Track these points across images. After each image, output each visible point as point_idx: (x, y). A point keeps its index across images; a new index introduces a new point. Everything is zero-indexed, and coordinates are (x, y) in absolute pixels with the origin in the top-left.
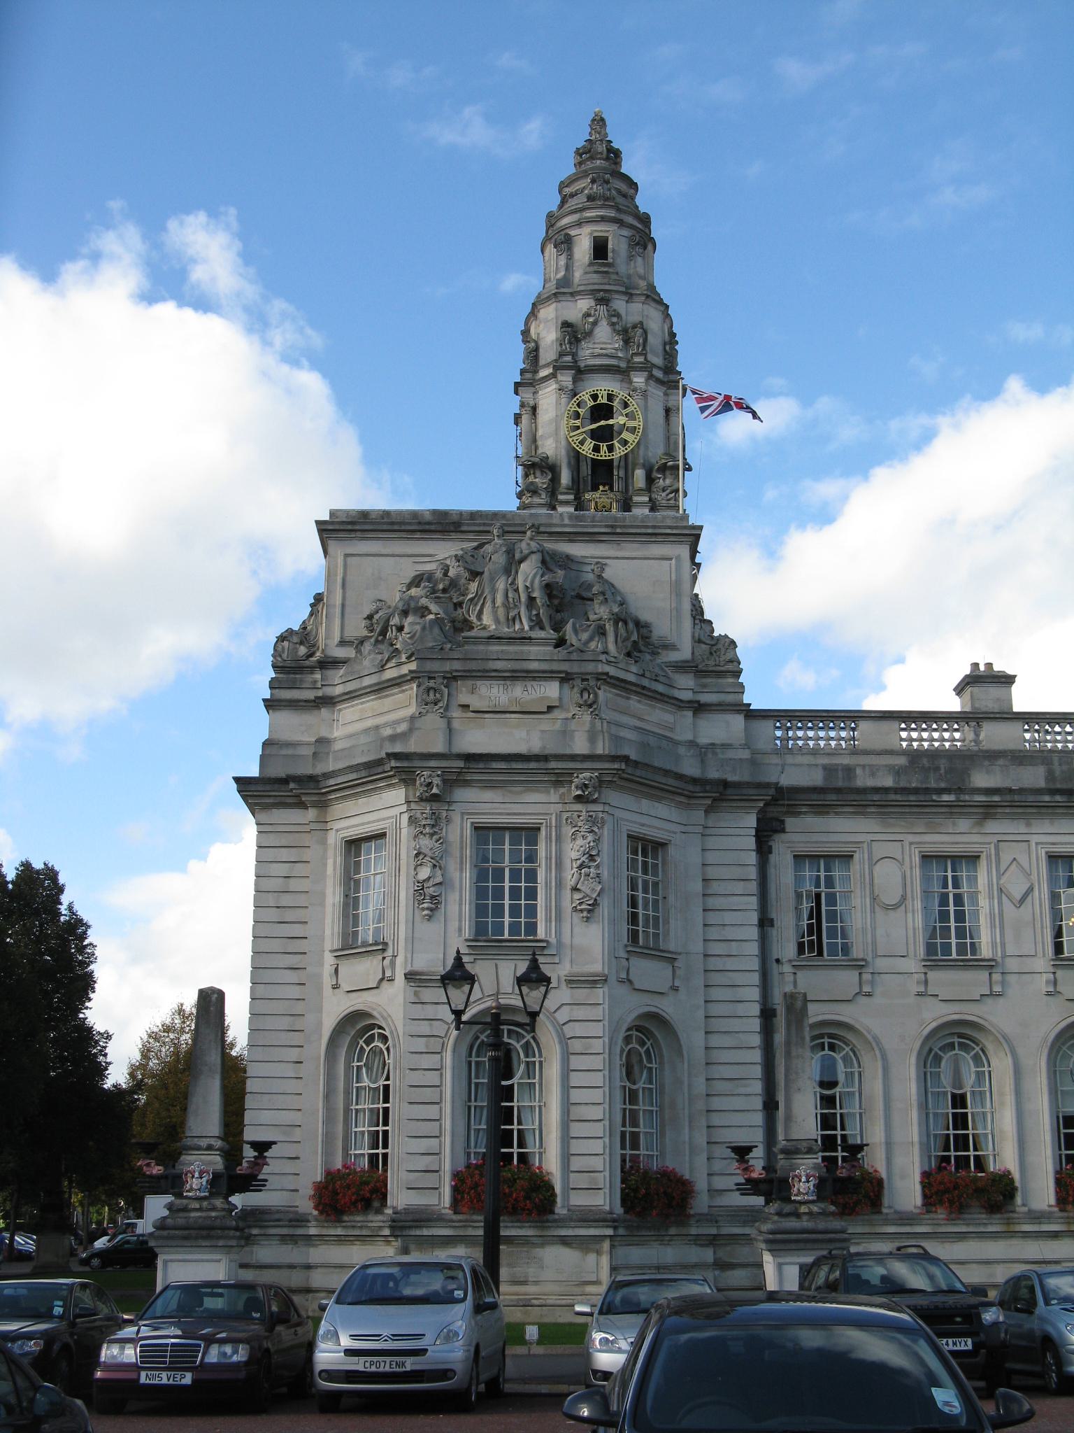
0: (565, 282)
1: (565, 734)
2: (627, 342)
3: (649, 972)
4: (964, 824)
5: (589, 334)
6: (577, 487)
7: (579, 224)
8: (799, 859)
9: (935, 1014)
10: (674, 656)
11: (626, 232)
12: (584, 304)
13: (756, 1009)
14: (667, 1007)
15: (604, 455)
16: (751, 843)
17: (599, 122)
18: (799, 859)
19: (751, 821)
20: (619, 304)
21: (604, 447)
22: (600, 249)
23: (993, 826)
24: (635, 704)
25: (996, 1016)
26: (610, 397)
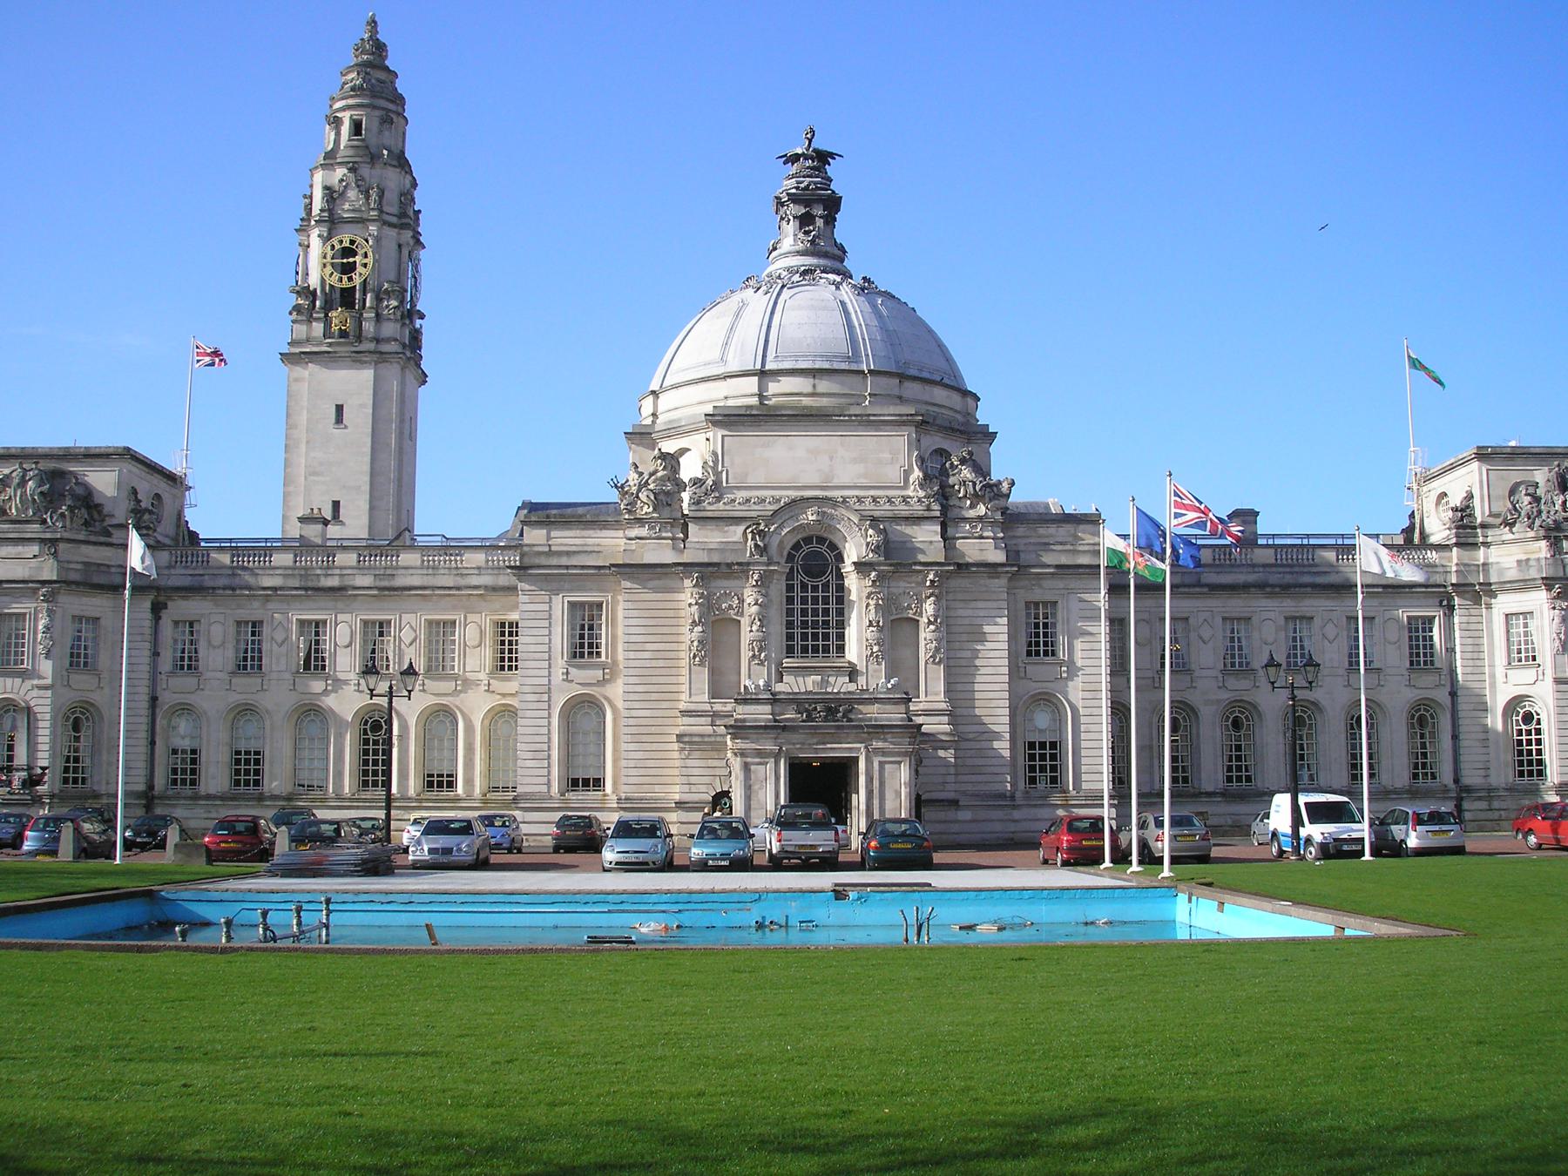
0: (330, 155)
1: (40, 569)
2: (368, 198)
3: (81, 680)
4: (256, 604)
5: (342, 194)
6: (328, 306)
7: (343, 109)
8: (176, 623)
9: (234, 698)
10: (115, 521)
11: (377, 113)
12: (341, 172)
13: (146, 698)
14: (97, 697)
15: (346, 284)
16: (149, 616)
17: (373, 23)
18: (176, 623)
19: (148, 605)
20: (365, 171)
21: (345, 278)
22: (357, 127)
23: (270, 606)
24: (84, 549)
25: (266, 701)
26: (352, 242)
